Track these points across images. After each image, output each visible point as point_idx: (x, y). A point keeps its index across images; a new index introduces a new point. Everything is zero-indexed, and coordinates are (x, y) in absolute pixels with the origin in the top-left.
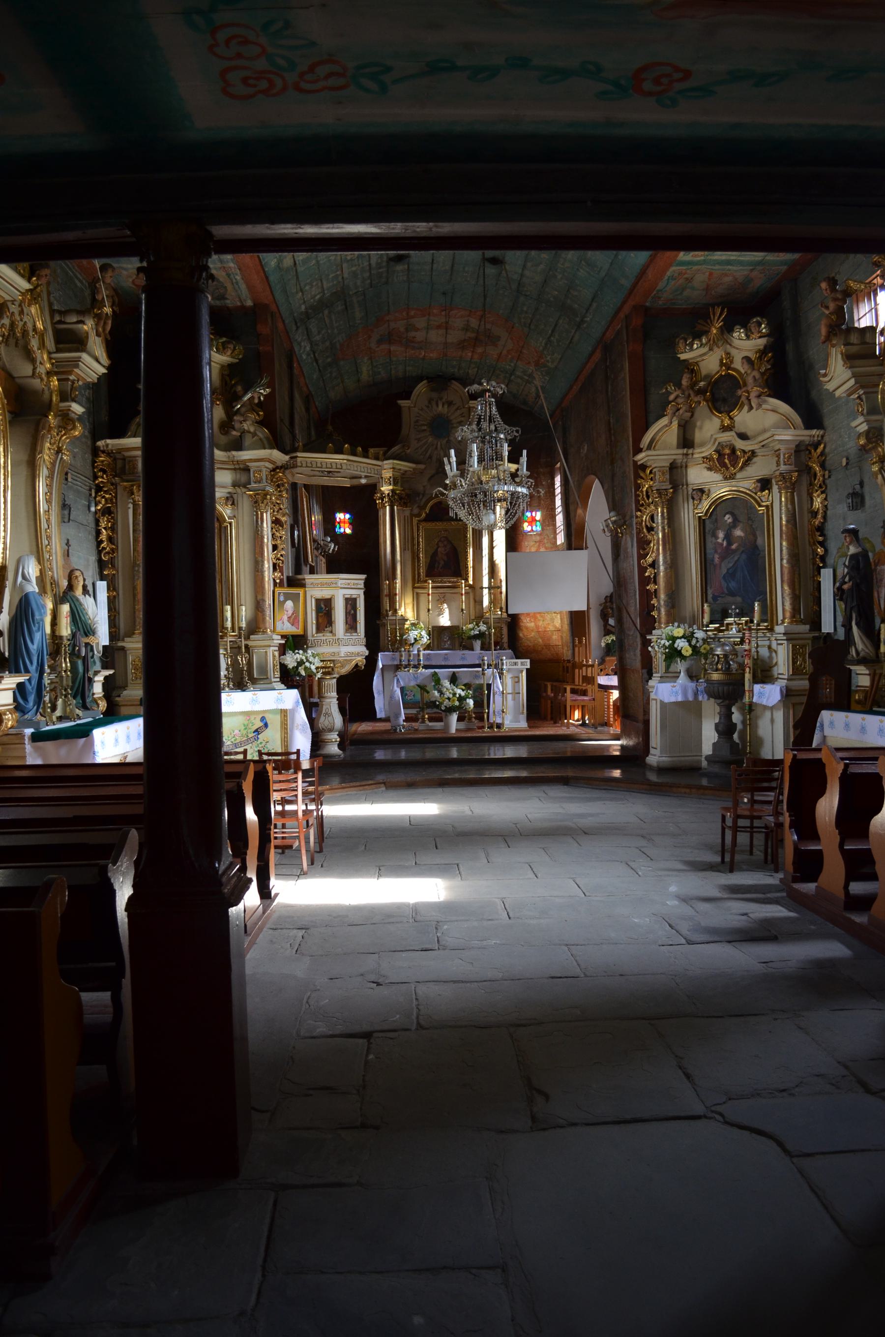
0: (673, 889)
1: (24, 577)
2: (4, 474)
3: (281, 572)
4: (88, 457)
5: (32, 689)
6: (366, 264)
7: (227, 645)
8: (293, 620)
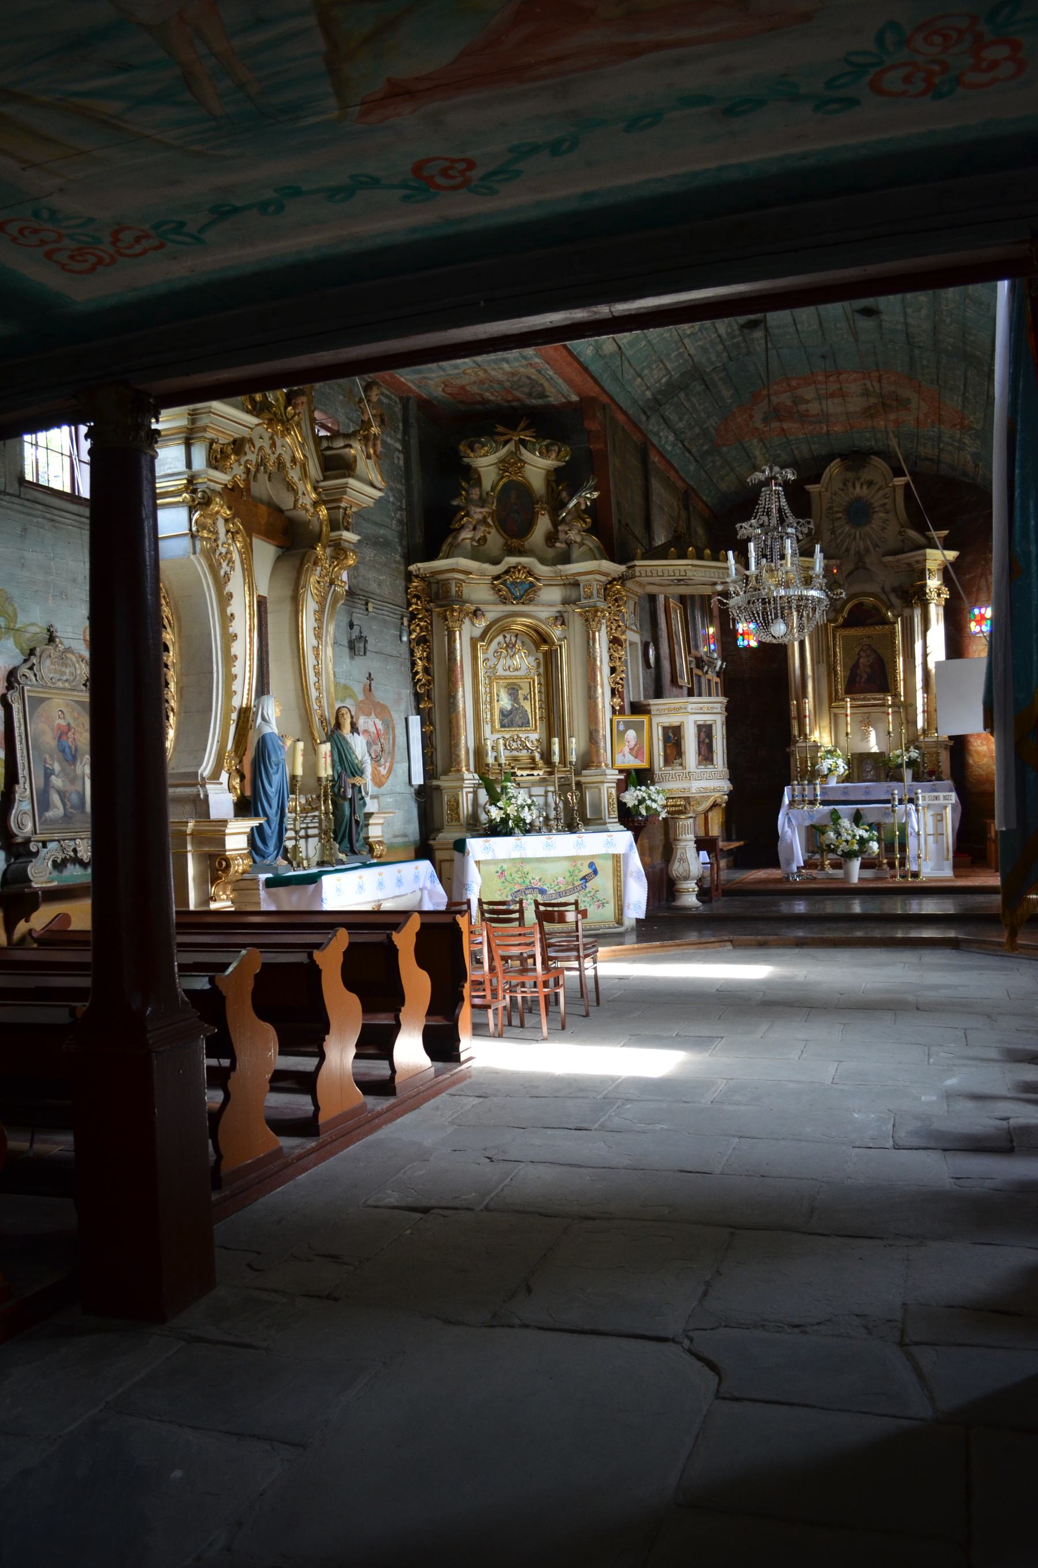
0: (951, 1082)
1: (263, 719)
2: (250, 614)
3: (621, 697)
4: (401, 583)
5: (272, 833)
6: (714, 336)
7: (554, 782)
8: (636, 751)
